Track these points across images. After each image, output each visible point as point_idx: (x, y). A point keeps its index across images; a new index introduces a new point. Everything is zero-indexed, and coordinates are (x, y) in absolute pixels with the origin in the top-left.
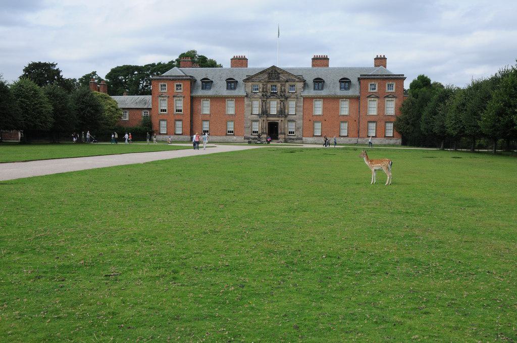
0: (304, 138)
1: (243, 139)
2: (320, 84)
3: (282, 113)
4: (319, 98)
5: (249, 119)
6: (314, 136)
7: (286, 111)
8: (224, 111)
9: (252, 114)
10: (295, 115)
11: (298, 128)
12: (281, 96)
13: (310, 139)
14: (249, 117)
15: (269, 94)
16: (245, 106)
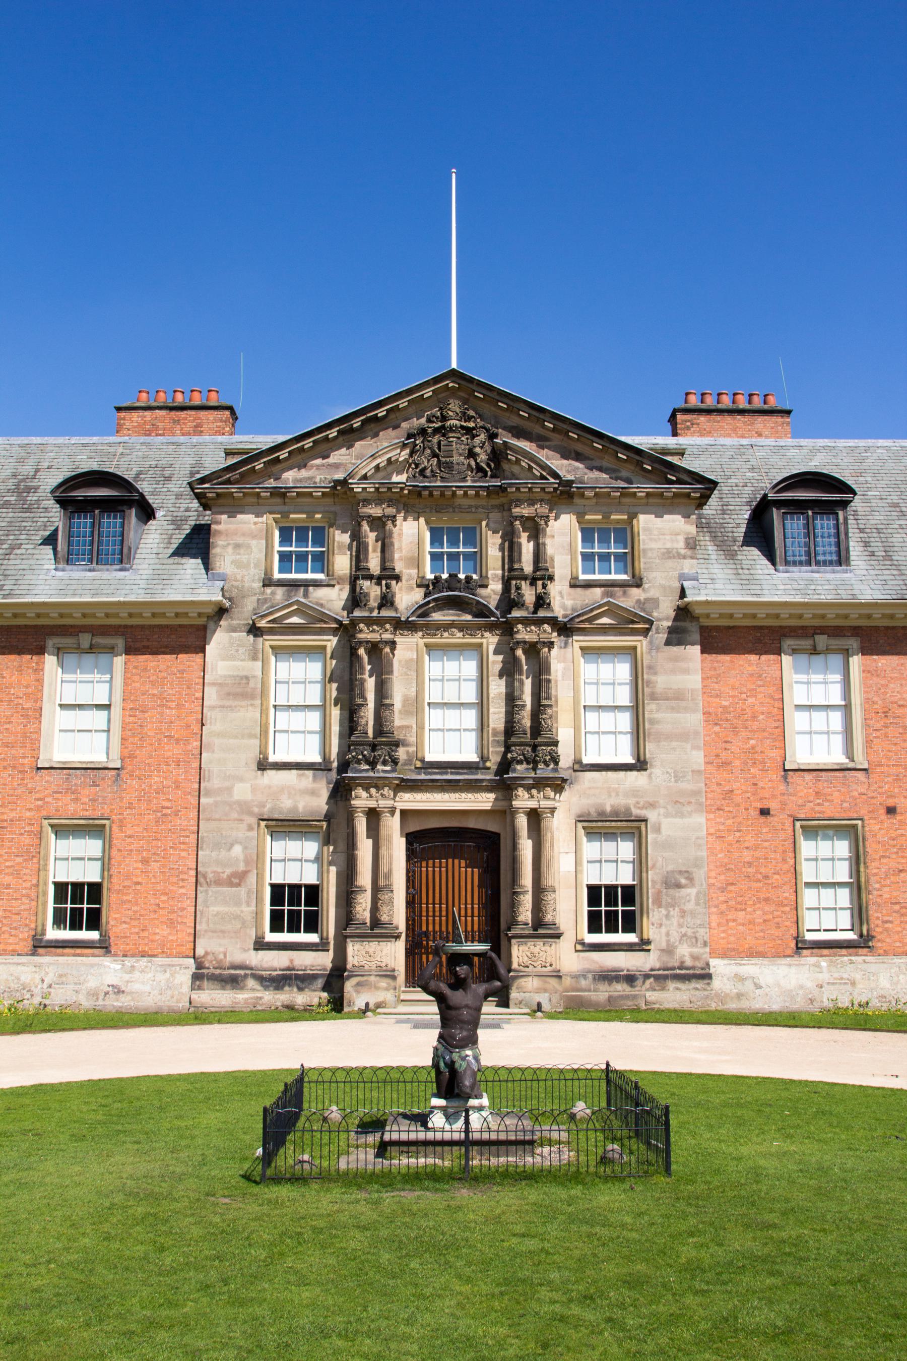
0: (718, 966)
1: (184, 978)
2: (823, 525)
3: (524, 749)
4: (836, 632)
5: (244, 808)
6: (801, 946)
7: (564, 734)
8: (32, 741)
9: (263, 765)
10: (640, 765)
11: (672, 883)
12: (518, 604)
13: (785, 980)
14: (242, 792)
15: (407, 598)
16: (211, 696)
